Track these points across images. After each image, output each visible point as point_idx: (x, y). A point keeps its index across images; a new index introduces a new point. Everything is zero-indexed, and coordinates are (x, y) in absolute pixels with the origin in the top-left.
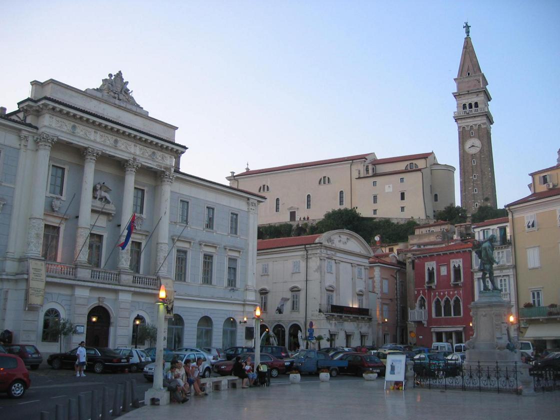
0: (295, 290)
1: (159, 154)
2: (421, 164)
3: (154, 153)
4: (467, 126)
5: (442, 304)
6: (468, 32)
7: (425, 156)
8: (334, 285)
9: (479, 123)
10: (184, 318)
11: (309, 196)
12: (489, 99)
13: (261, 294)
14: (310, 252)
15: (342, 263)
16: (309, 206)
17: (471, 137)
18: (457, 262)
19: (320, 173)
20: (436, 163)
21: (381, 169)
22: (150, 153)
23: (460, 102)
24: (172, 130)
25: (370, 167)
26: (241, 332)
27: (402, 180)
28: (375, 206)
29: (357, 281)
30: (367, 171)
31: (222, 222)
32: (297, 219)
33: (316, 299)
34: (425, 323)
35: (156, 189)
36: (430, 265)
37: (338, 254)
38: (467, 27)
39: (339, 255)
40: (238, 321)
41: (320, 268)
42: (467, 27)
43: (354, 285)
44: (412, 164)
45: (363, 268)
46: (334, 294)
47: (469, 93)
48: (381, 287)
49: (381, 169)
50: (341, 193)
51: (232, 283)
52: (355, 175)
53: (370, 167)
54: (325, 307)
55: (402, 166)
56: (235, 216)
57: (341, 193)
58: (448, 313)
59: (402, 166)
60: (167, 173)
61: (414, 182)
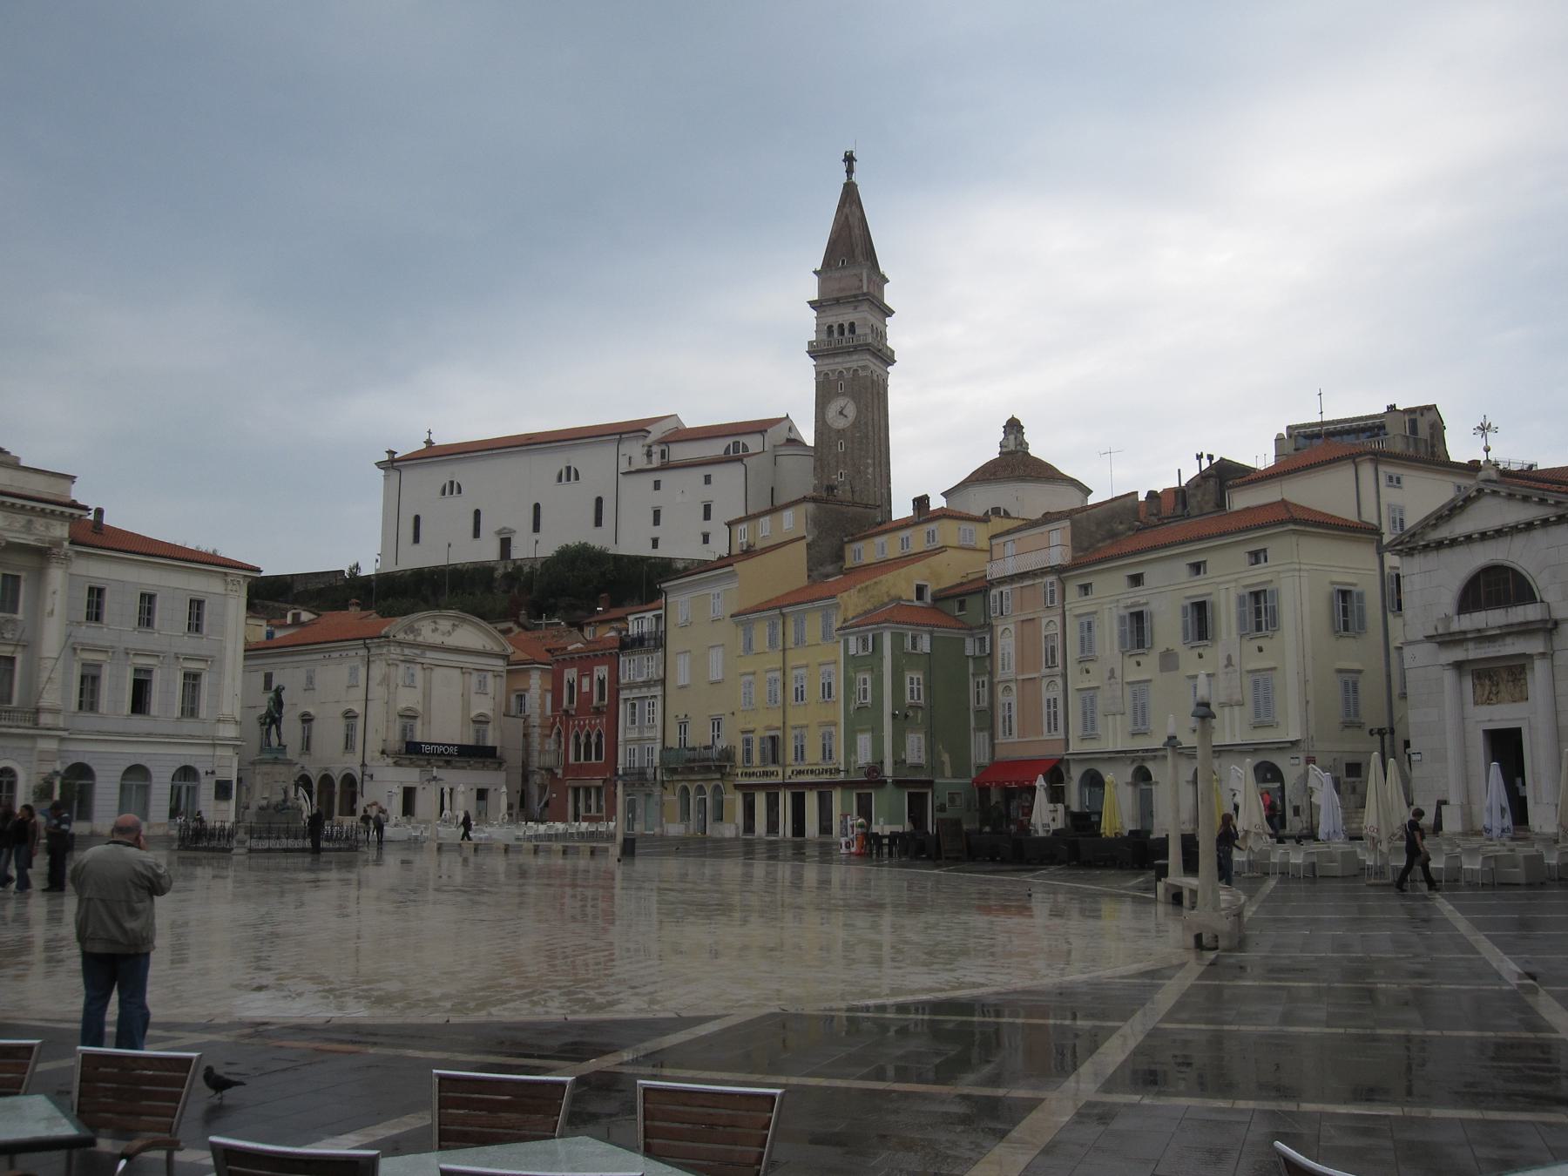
0: (349, 716)
1: (39, 524)
2: (753, 443)
3: (30, 521)
4: (833, 371)
5: (583, 739)
6: (850, 171)
7: (759, 428)
8: (420, 708)
9: (854, 365)
10: (94, 768)
11: (537, 507)
12: (888, 312)
13: (304, 721)
14: (373, 651)
15: (438, 671)
16: (536, 528)
17: (838, 395)
18: (602, 671)
19: (557, 461)
20: (792, 436)
21: (679, 452)
22: (23, 522)
23: (824, 320)
24: (67, 482)
25: (656, 449)
26: (206, 789)
27: (708, 479)
28: (656, 532)
29: (475, 699)
30: (649, 455)
31: (171, 615)
32: (515, 555)
33: (381, 731)
34: (559, 772)
35: (40, 575)
36: (571, 674)
37: (429, 654)
38: (849, 159)
39: (431, 655)
40: (202, 772)
41: (385, 680)
42: (849, 159)
43: (466, 706)
44: (736, 441)
45: (490, 675)
46: (419, 723)
47: (837, 301)
48: (542, 706)
49: (679, 452)
50: (599, 501)
51: (190, 709)
52: (624, 467)
53: (656, 449)
54: (395, 741)
55: (717, 448)
56: (197, 606)
57: (599, 501)
58: (588, 757)
59: (717, 448)
60: (55, 550)
61: (729, 479)
